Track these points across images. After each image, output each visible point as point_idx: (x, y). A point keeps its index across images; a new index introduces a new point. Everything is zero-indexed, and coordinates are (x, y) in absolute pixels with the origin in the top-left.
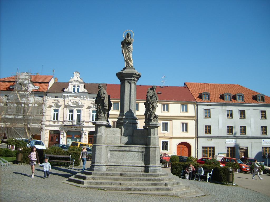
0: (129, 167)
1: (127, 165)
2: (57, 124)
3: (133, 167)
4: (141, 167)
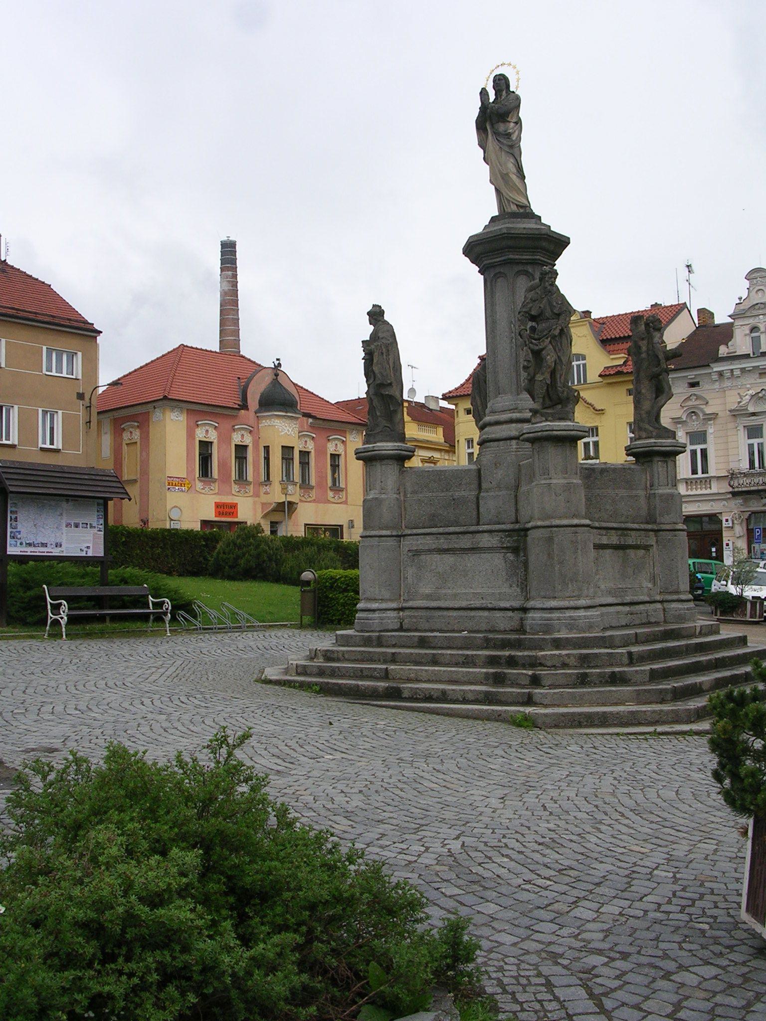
0: (473, 613)
1: (464, 604)
2: (708, 491)
3: (486, 613)
4: (510, 614)
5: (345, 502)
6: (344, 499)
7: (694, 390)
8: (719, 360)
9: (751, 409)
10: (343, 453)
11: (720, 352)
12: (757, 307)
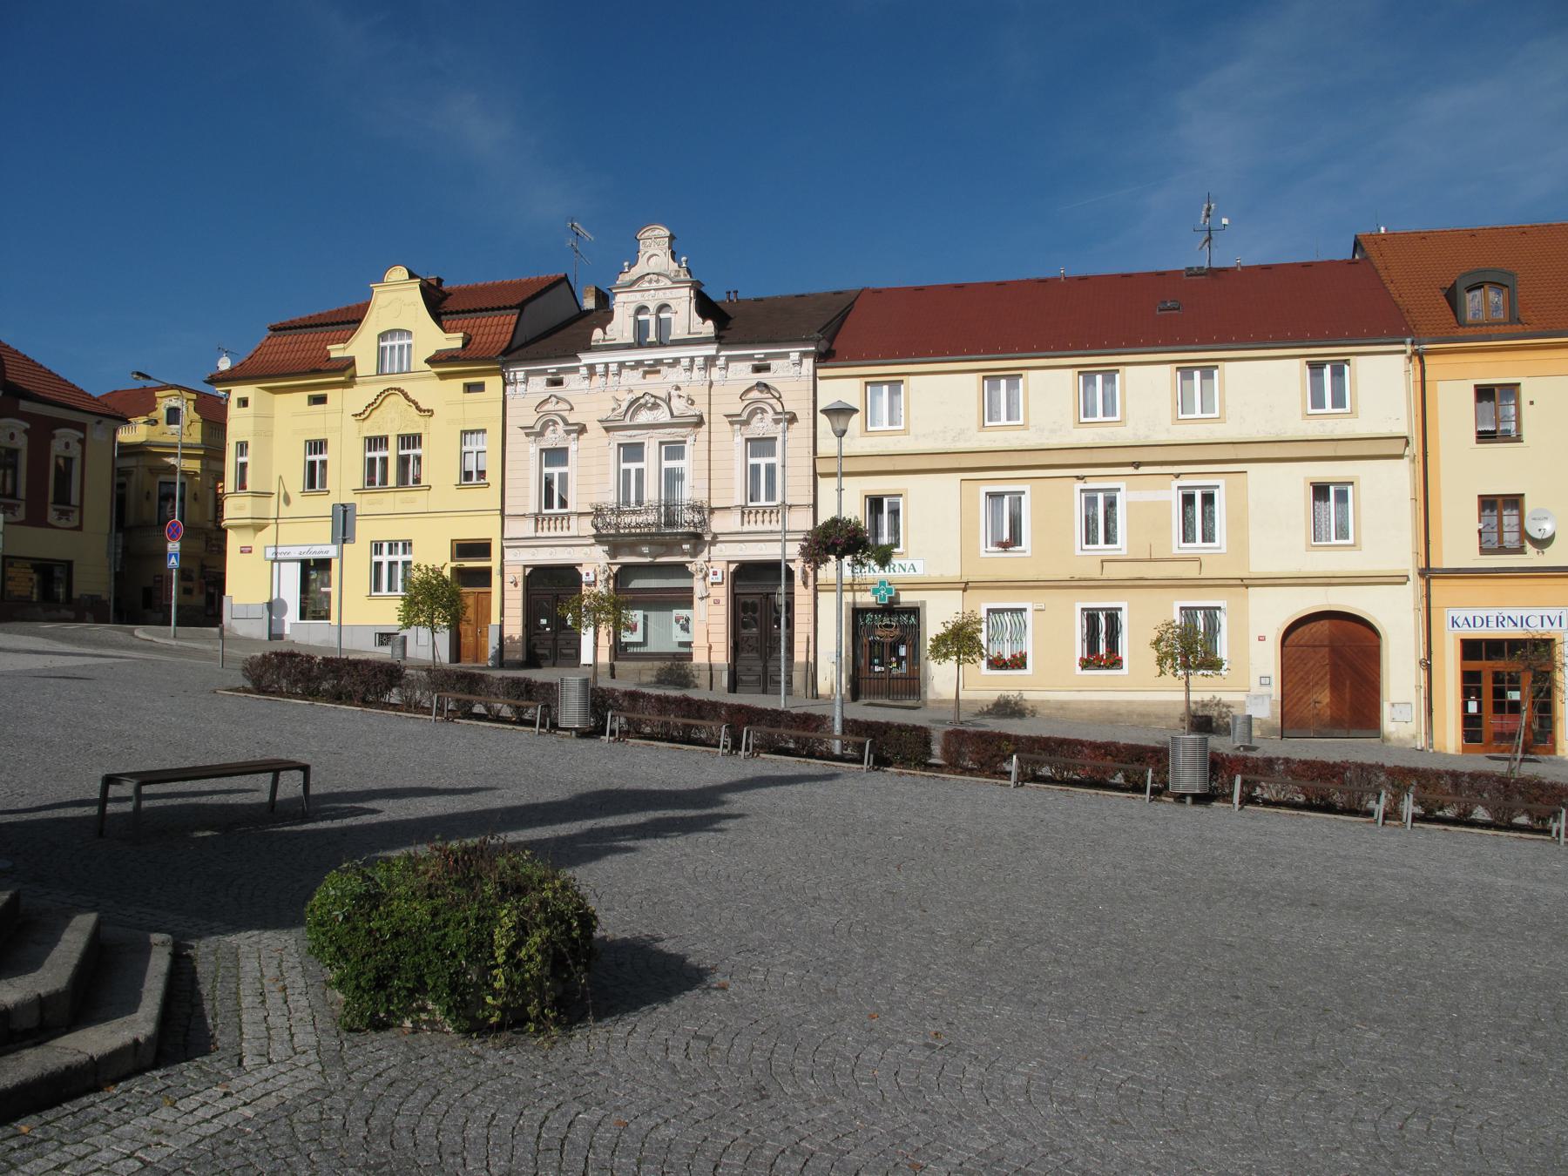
2: (565, 533)
5: (79, 528)
6: (77, 523)
7: (555, 390)
8: (589, 349)
9: (627, 422)
10: (79, 456)
11: (594, 338)
12: (647, 278)
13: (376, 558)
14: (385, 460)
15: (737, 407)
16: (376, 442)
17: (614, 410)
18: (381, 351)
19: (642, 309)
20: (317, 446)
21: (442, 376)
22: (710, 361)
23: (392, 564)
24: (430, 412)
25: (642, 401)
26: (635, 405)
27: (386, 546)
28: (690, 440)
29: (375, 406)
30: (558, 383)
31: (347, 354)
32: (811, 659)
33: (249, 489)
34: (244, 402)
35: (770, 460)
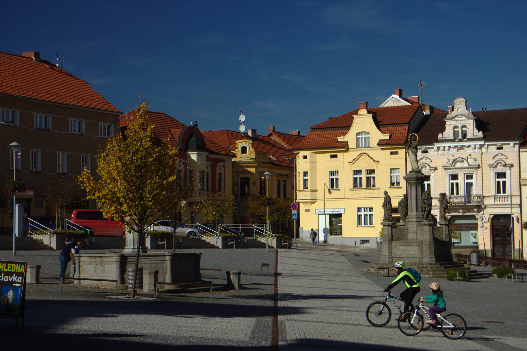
8: (437, 141)
9: (453, 167)
12: (458, 116)
13: (359, 213)
14: (361, 179)
15: (492, 162)
16: (356, 172)
17: (447, 163)
18: (357, 139)
19: (456, 127)
20: (333, 173)
21: (382, 149)
22: (481, 146)
23: (365, 215)
24: (378, 162)
25: (458, 160)
26: (455, 161)
27: (363, 209)
28: (475, 173)
29: (357, 159)
30: (426, 152)
31: (345, 140)
32: (521, 247)
33: (309, 188)
34: (305, 157)
35: (504, 180)
